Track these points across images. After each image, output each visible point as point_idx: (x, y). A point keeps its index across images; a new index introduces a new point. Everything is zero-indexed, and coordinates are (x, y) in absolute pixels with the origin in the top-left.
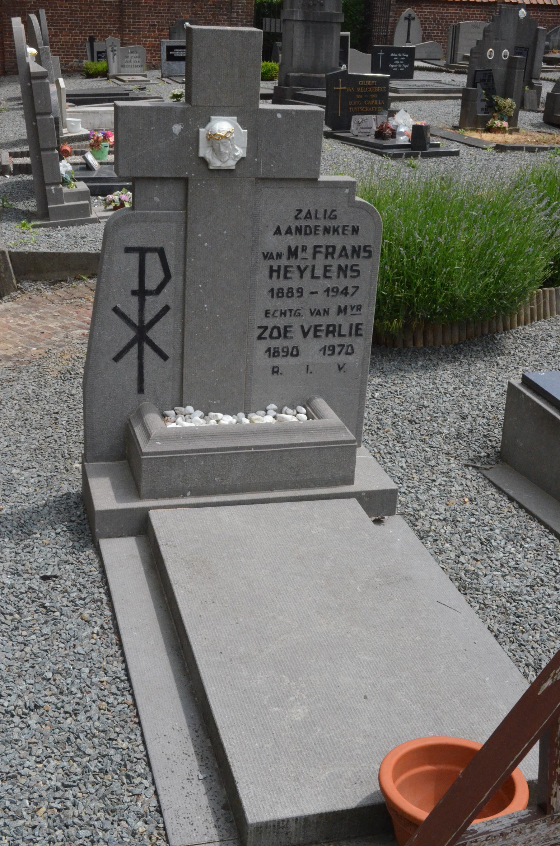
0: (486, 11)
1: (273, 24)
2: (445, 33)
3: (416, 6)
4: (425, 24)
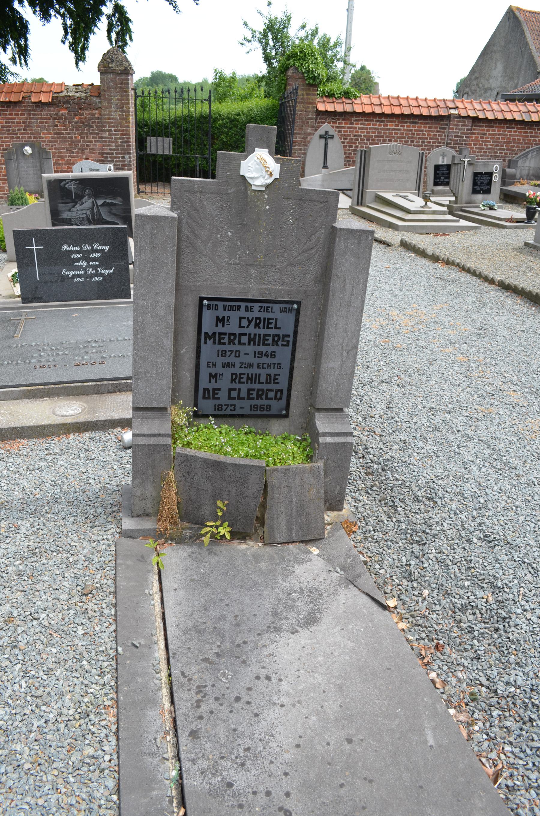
0: (435, 128)
1: (160, 144)
3: (343, 120)
4: (355, 143)
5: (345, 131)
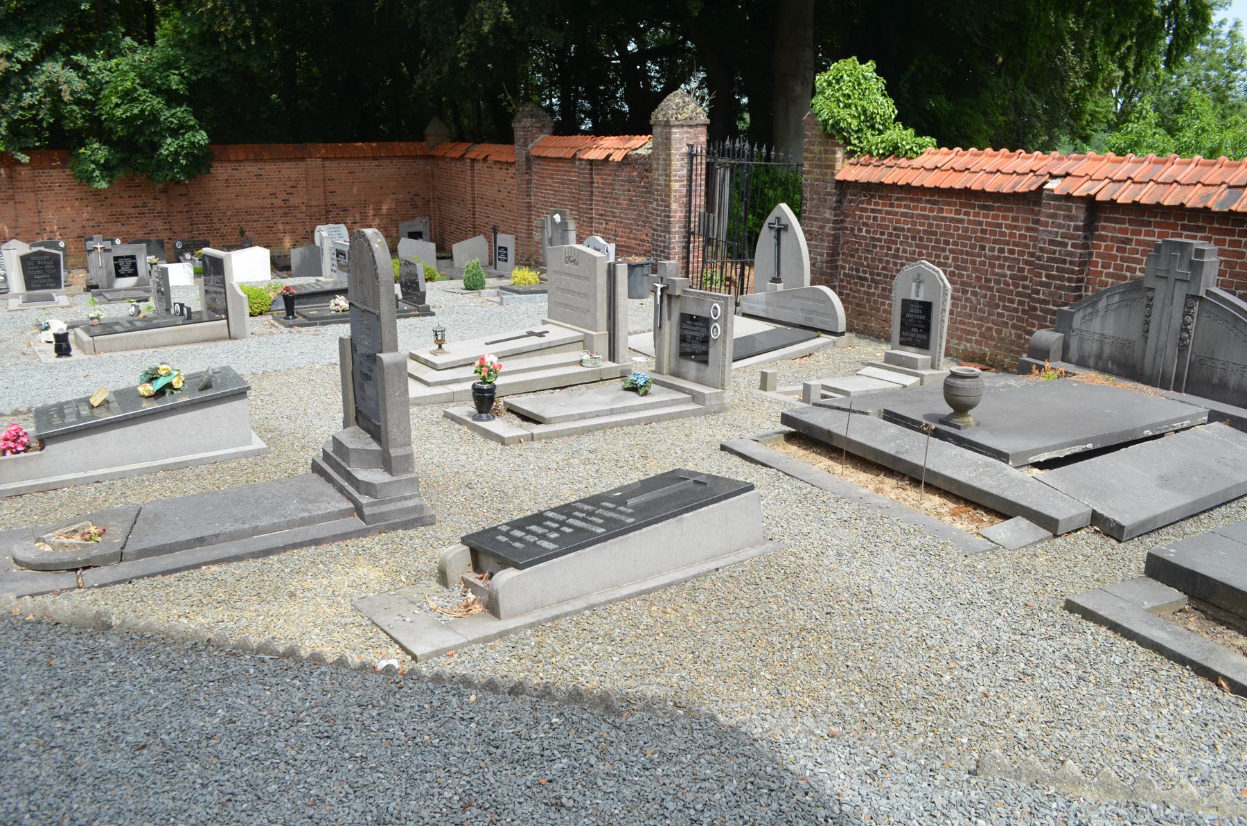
3: (881, 197)
5: (883, 219)
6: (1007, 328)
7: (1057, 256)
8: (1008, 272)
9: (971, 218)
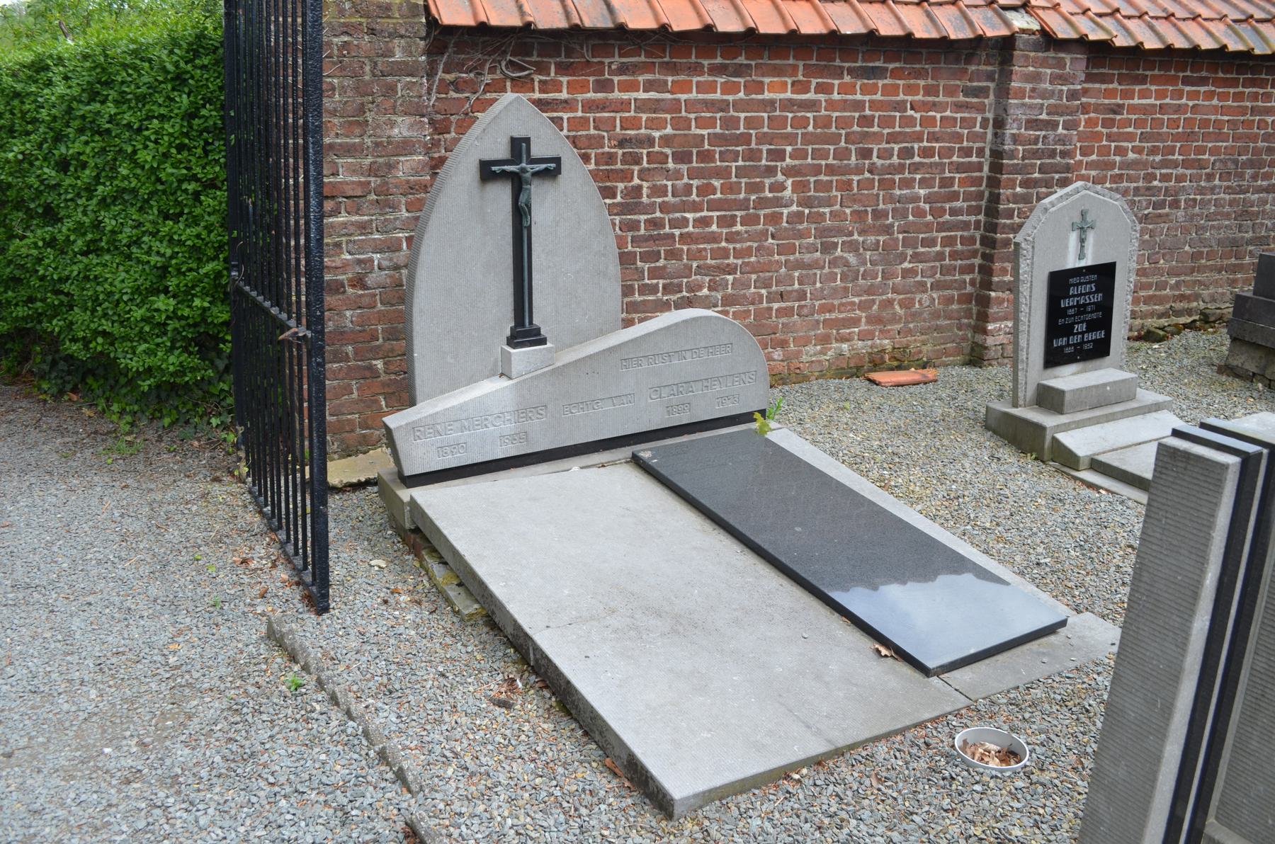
0: (950, 92)
2: (749, 220)
3: (563, 69)
4: (627, 176)
6: (925, 291)
7: (1040, 145)
8: (922, 192)
9: (836, 96)
